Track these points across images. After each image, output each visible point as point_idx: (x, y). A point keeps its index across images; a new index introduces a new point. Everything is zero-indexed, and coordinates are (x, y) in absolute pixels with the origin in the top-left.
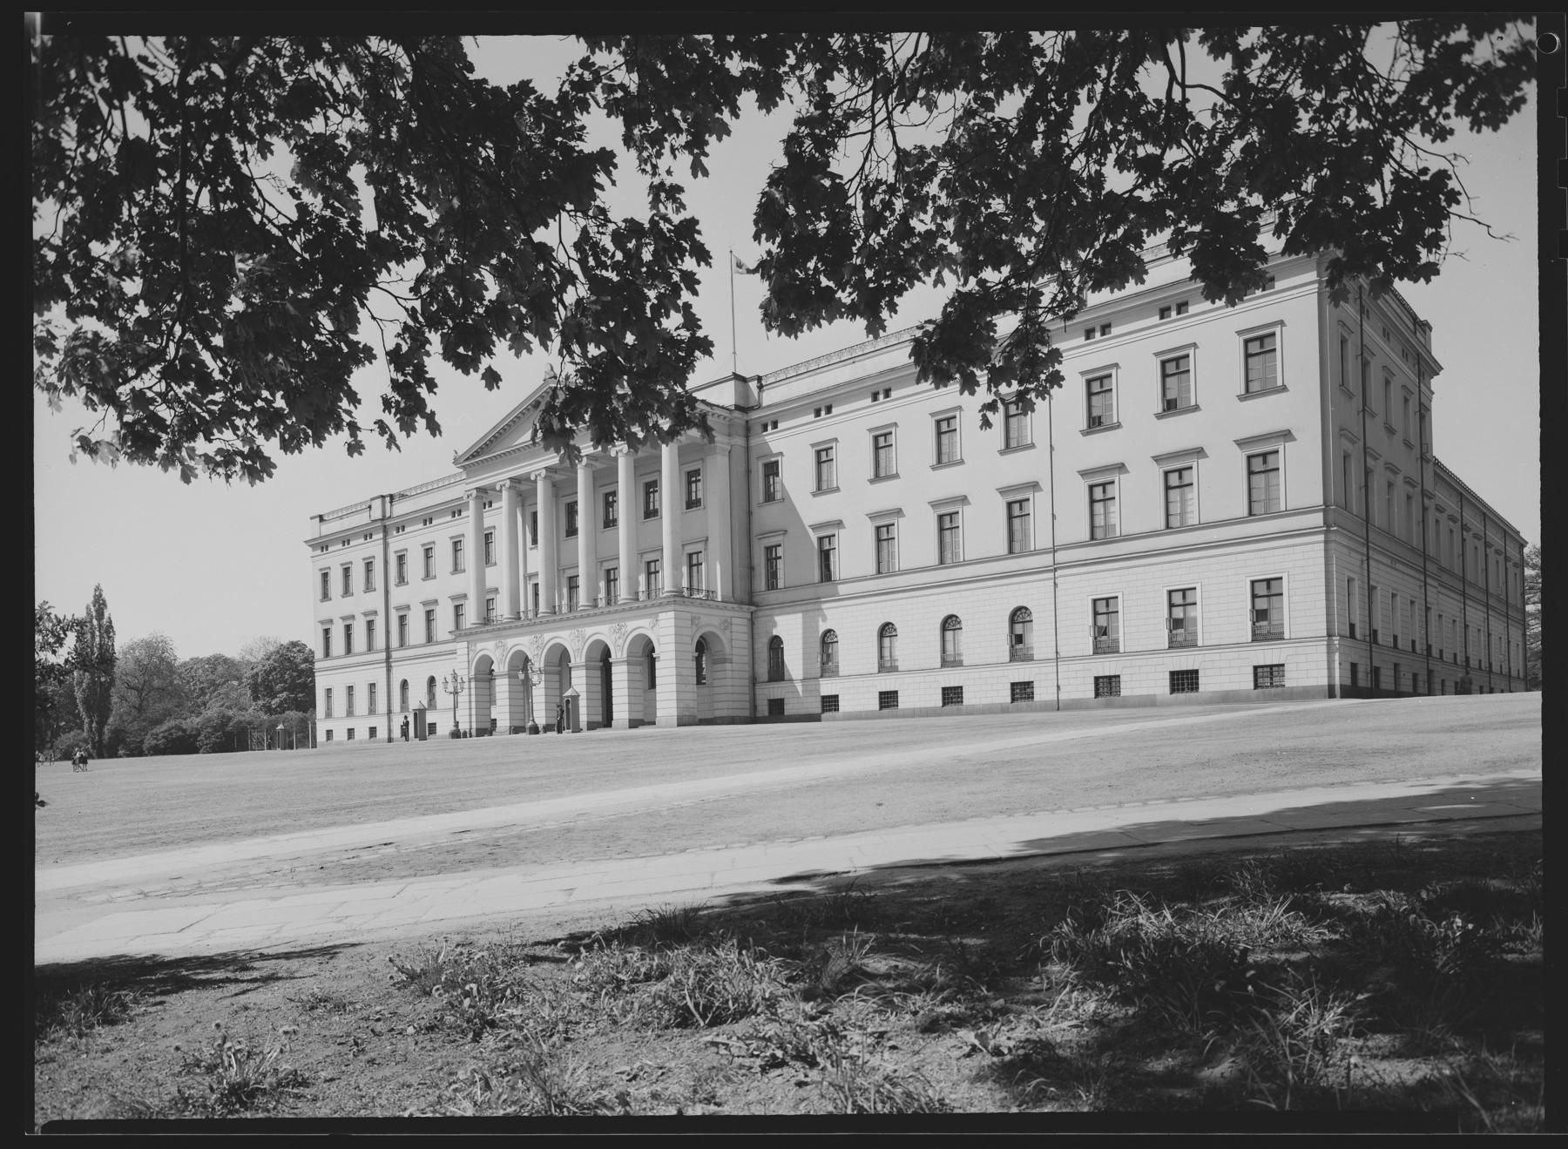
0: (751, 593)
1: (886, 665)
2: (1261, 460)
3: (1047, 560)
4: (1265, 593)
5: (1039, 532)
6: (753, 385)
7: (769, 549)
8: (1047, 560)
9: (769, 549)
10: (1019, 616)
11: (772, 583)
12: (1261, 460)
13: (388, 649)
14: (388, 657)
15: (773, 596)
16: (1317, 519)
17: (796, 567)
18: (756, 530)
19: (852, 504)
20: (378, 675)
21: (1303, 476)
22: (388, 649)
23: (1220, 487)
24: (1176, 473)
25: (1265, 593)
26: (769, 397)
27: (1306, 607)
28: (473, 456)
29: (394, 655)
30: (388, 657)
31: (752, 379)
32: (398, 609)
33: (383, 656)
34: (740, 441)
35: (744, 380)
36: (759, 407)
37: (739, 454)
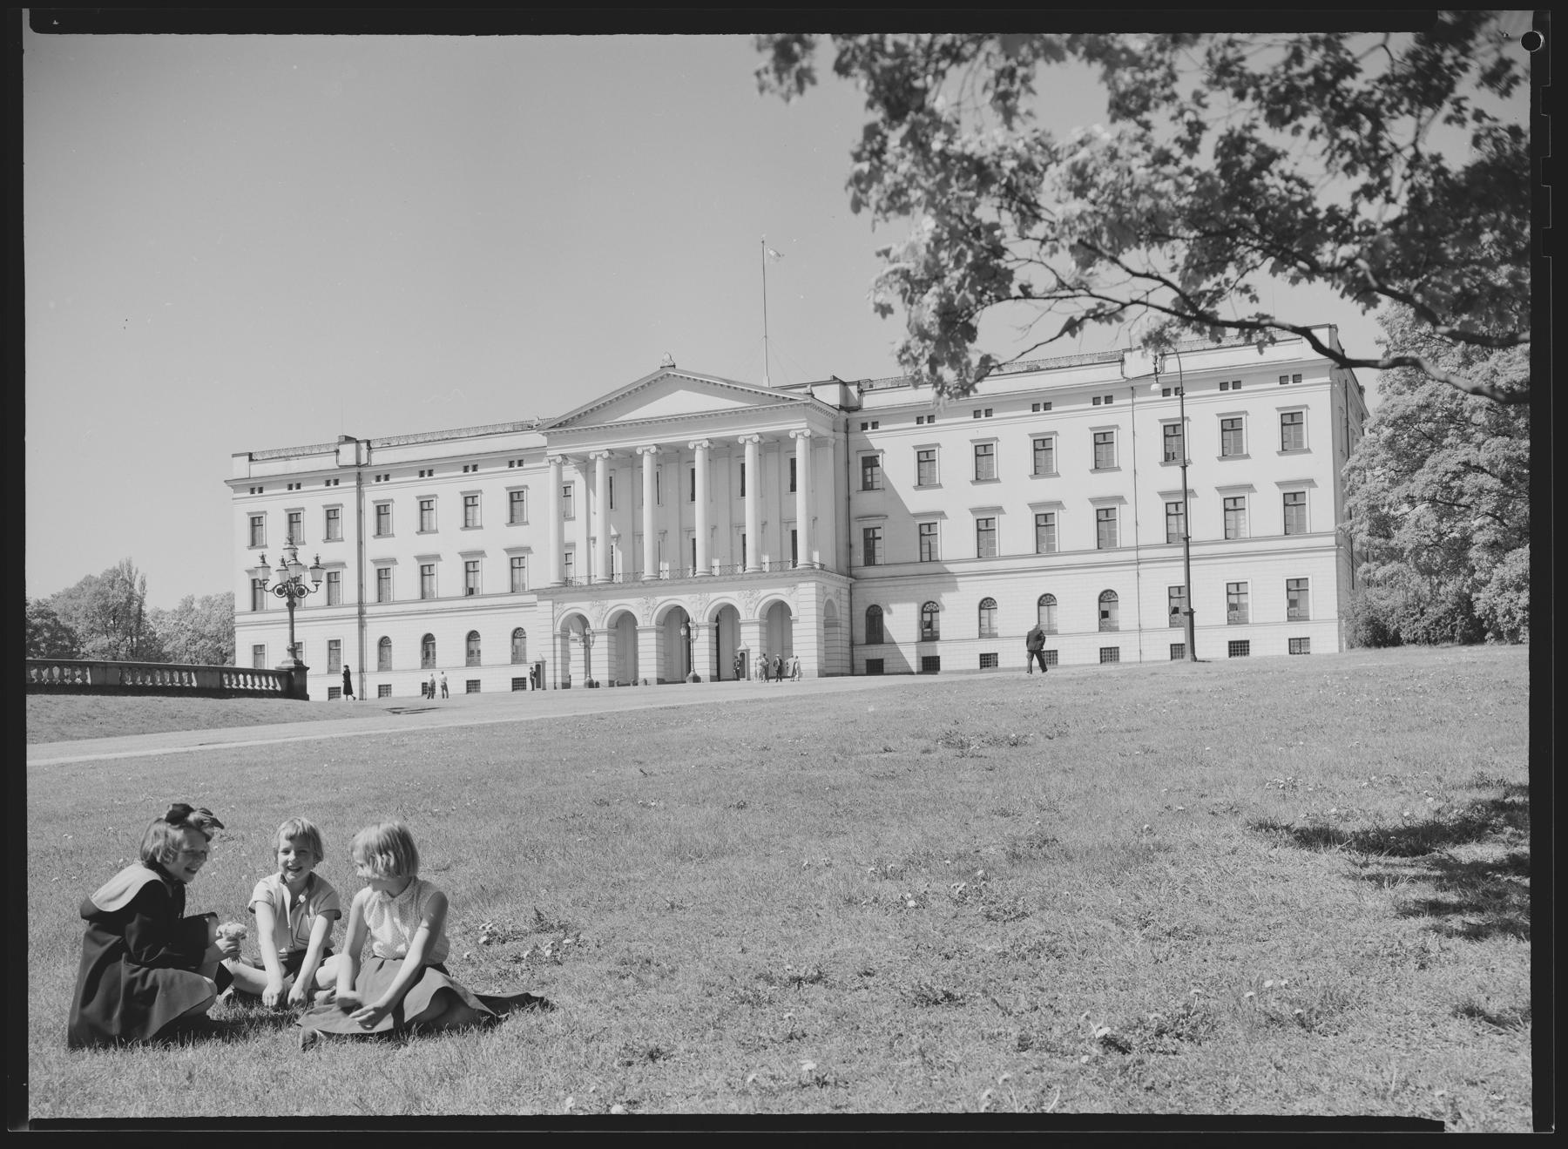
0: (850, 567)
1: (985, 633)
2: (1293, 500)
3: (1132, 555)
4: (1296, 589)
5: (1125, 533)
6: (853, 389)
7: (866, 531)
8: (1132, 555)
9: (866, 531)
10: (1107, 597)
11: (870, 559)
12: (1293, 500)
13: (361, 603)
14: (361, 613)
15: (871, 571)
16: (1331, 541)
17: (895, 546)
18: (854, 513)
19: (954, 500)
20: (347, 632)
21: (1321, 511)
22: (361, 603)
23: (1264, 513)
24: (1233, 503)
25: (1296, 589)
26: (869, 401)
27: (1325, 598)
28: (561, 425)
29: (369, 610)
30: (361, 613)
31: (852, 383)
32: (375, 562)
33: (355, 610)
34: (842, 436)
35: (844, 384)
36: (858, 408)
37: (842, 445)
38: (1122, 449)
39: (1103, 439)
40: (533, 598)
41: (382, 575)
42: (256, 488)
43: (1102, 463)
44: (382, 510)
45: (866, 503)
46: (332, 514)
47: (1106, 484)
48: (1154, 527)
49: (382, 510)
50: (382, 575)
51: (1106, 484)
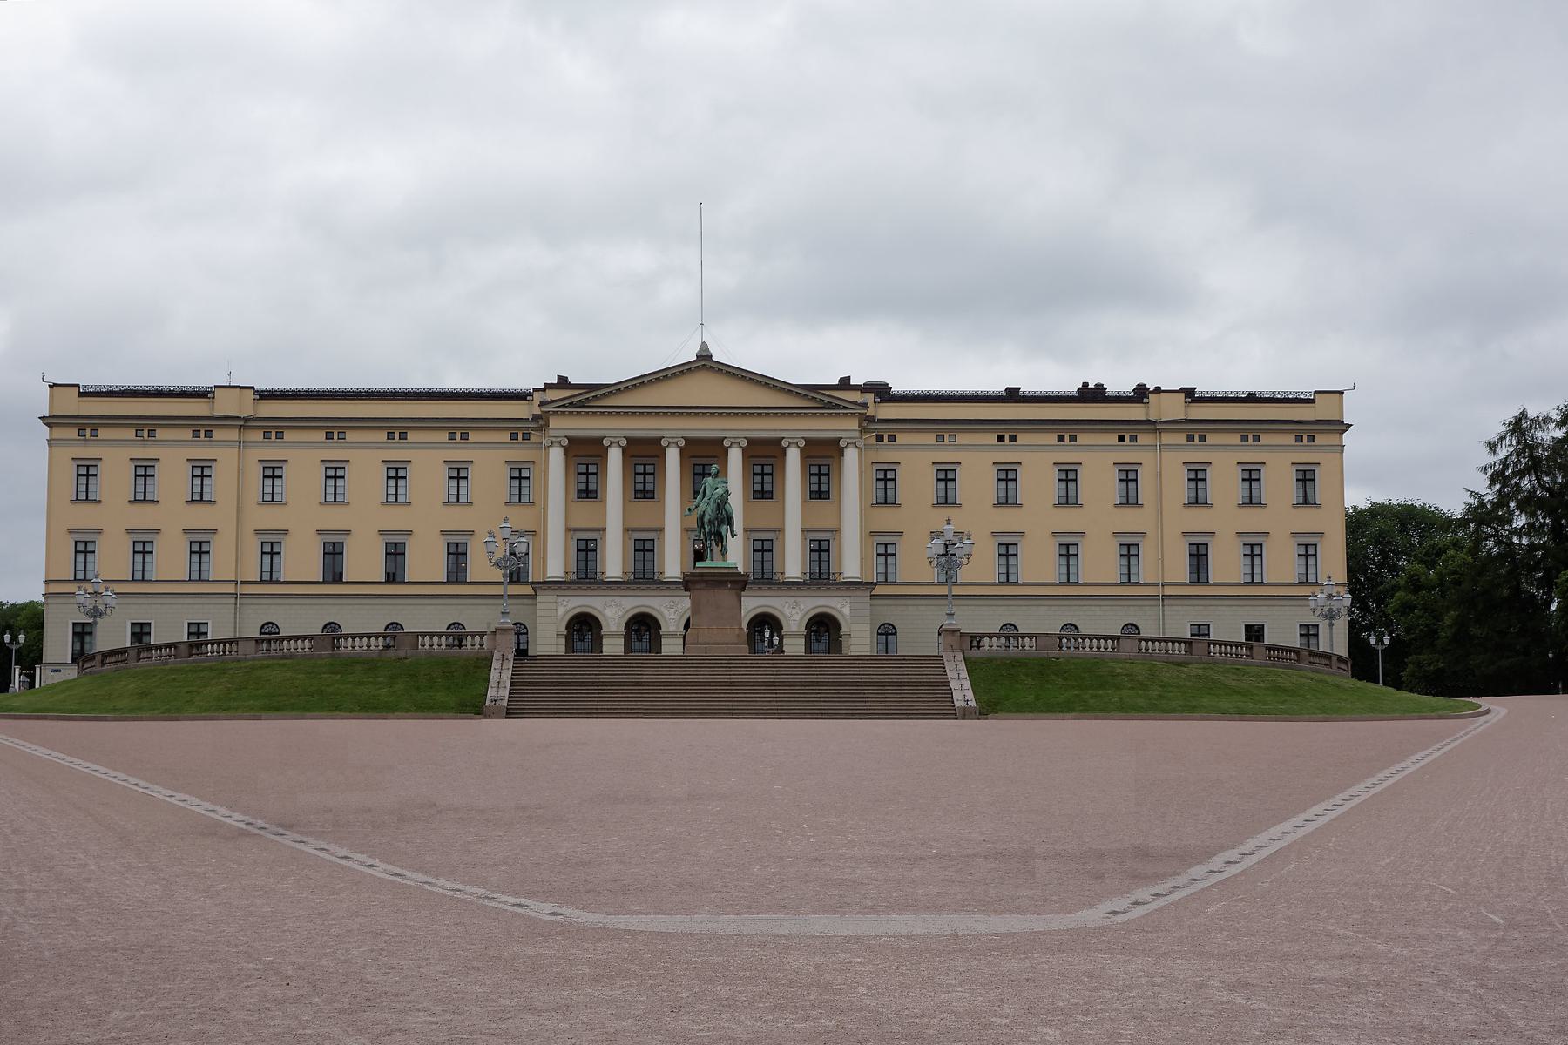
5: (1147, 570)
32: (258, 532)
38: (1145, 487)
39: (1128, 477)
40: (528, 590)
41: (271, 551)
42: (87, 426)
43: (1129, 500)
44: (272, 472)
45: (887, 519)
46: (201, 472)
47: (1130, 520)
48: (1180, 569)
49: (272, 472)
50: (271, 551)
51: (1130, 520)
